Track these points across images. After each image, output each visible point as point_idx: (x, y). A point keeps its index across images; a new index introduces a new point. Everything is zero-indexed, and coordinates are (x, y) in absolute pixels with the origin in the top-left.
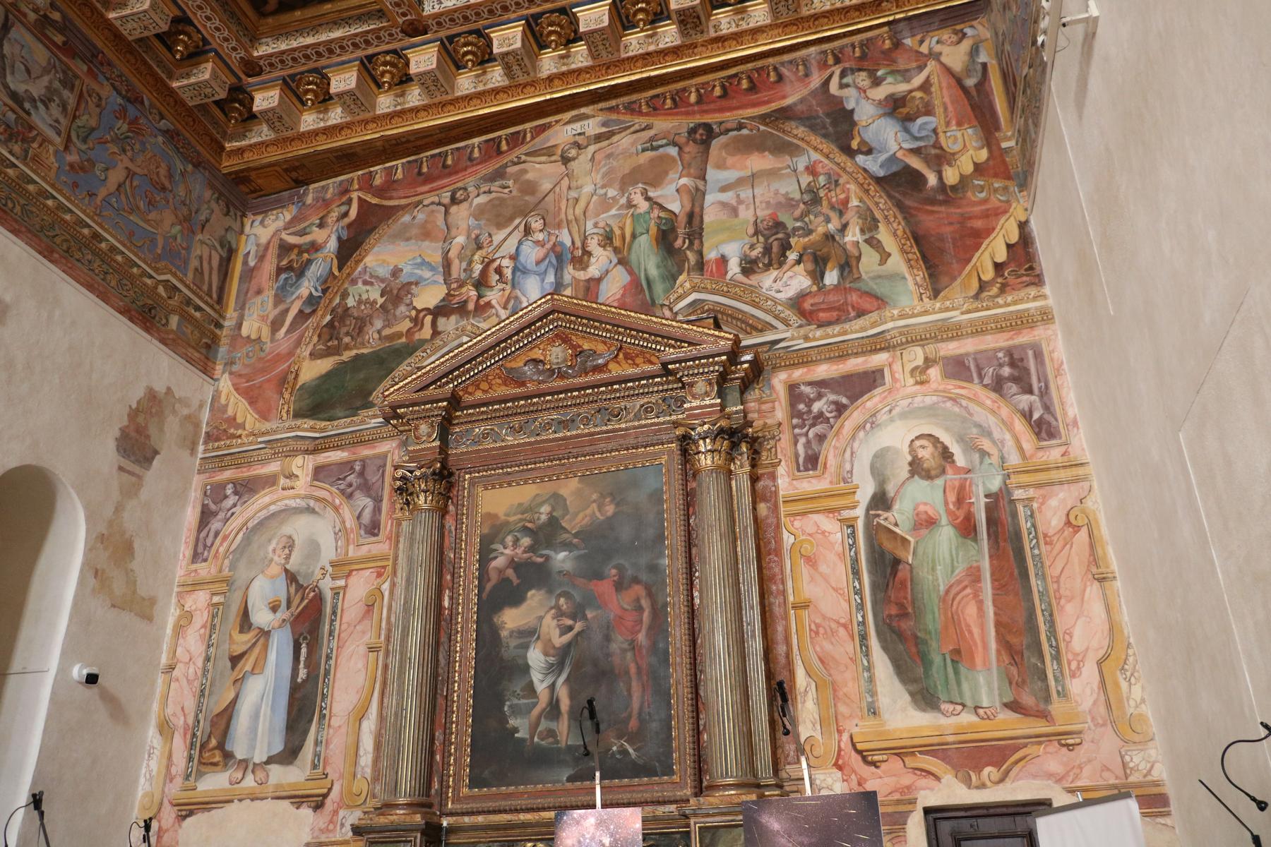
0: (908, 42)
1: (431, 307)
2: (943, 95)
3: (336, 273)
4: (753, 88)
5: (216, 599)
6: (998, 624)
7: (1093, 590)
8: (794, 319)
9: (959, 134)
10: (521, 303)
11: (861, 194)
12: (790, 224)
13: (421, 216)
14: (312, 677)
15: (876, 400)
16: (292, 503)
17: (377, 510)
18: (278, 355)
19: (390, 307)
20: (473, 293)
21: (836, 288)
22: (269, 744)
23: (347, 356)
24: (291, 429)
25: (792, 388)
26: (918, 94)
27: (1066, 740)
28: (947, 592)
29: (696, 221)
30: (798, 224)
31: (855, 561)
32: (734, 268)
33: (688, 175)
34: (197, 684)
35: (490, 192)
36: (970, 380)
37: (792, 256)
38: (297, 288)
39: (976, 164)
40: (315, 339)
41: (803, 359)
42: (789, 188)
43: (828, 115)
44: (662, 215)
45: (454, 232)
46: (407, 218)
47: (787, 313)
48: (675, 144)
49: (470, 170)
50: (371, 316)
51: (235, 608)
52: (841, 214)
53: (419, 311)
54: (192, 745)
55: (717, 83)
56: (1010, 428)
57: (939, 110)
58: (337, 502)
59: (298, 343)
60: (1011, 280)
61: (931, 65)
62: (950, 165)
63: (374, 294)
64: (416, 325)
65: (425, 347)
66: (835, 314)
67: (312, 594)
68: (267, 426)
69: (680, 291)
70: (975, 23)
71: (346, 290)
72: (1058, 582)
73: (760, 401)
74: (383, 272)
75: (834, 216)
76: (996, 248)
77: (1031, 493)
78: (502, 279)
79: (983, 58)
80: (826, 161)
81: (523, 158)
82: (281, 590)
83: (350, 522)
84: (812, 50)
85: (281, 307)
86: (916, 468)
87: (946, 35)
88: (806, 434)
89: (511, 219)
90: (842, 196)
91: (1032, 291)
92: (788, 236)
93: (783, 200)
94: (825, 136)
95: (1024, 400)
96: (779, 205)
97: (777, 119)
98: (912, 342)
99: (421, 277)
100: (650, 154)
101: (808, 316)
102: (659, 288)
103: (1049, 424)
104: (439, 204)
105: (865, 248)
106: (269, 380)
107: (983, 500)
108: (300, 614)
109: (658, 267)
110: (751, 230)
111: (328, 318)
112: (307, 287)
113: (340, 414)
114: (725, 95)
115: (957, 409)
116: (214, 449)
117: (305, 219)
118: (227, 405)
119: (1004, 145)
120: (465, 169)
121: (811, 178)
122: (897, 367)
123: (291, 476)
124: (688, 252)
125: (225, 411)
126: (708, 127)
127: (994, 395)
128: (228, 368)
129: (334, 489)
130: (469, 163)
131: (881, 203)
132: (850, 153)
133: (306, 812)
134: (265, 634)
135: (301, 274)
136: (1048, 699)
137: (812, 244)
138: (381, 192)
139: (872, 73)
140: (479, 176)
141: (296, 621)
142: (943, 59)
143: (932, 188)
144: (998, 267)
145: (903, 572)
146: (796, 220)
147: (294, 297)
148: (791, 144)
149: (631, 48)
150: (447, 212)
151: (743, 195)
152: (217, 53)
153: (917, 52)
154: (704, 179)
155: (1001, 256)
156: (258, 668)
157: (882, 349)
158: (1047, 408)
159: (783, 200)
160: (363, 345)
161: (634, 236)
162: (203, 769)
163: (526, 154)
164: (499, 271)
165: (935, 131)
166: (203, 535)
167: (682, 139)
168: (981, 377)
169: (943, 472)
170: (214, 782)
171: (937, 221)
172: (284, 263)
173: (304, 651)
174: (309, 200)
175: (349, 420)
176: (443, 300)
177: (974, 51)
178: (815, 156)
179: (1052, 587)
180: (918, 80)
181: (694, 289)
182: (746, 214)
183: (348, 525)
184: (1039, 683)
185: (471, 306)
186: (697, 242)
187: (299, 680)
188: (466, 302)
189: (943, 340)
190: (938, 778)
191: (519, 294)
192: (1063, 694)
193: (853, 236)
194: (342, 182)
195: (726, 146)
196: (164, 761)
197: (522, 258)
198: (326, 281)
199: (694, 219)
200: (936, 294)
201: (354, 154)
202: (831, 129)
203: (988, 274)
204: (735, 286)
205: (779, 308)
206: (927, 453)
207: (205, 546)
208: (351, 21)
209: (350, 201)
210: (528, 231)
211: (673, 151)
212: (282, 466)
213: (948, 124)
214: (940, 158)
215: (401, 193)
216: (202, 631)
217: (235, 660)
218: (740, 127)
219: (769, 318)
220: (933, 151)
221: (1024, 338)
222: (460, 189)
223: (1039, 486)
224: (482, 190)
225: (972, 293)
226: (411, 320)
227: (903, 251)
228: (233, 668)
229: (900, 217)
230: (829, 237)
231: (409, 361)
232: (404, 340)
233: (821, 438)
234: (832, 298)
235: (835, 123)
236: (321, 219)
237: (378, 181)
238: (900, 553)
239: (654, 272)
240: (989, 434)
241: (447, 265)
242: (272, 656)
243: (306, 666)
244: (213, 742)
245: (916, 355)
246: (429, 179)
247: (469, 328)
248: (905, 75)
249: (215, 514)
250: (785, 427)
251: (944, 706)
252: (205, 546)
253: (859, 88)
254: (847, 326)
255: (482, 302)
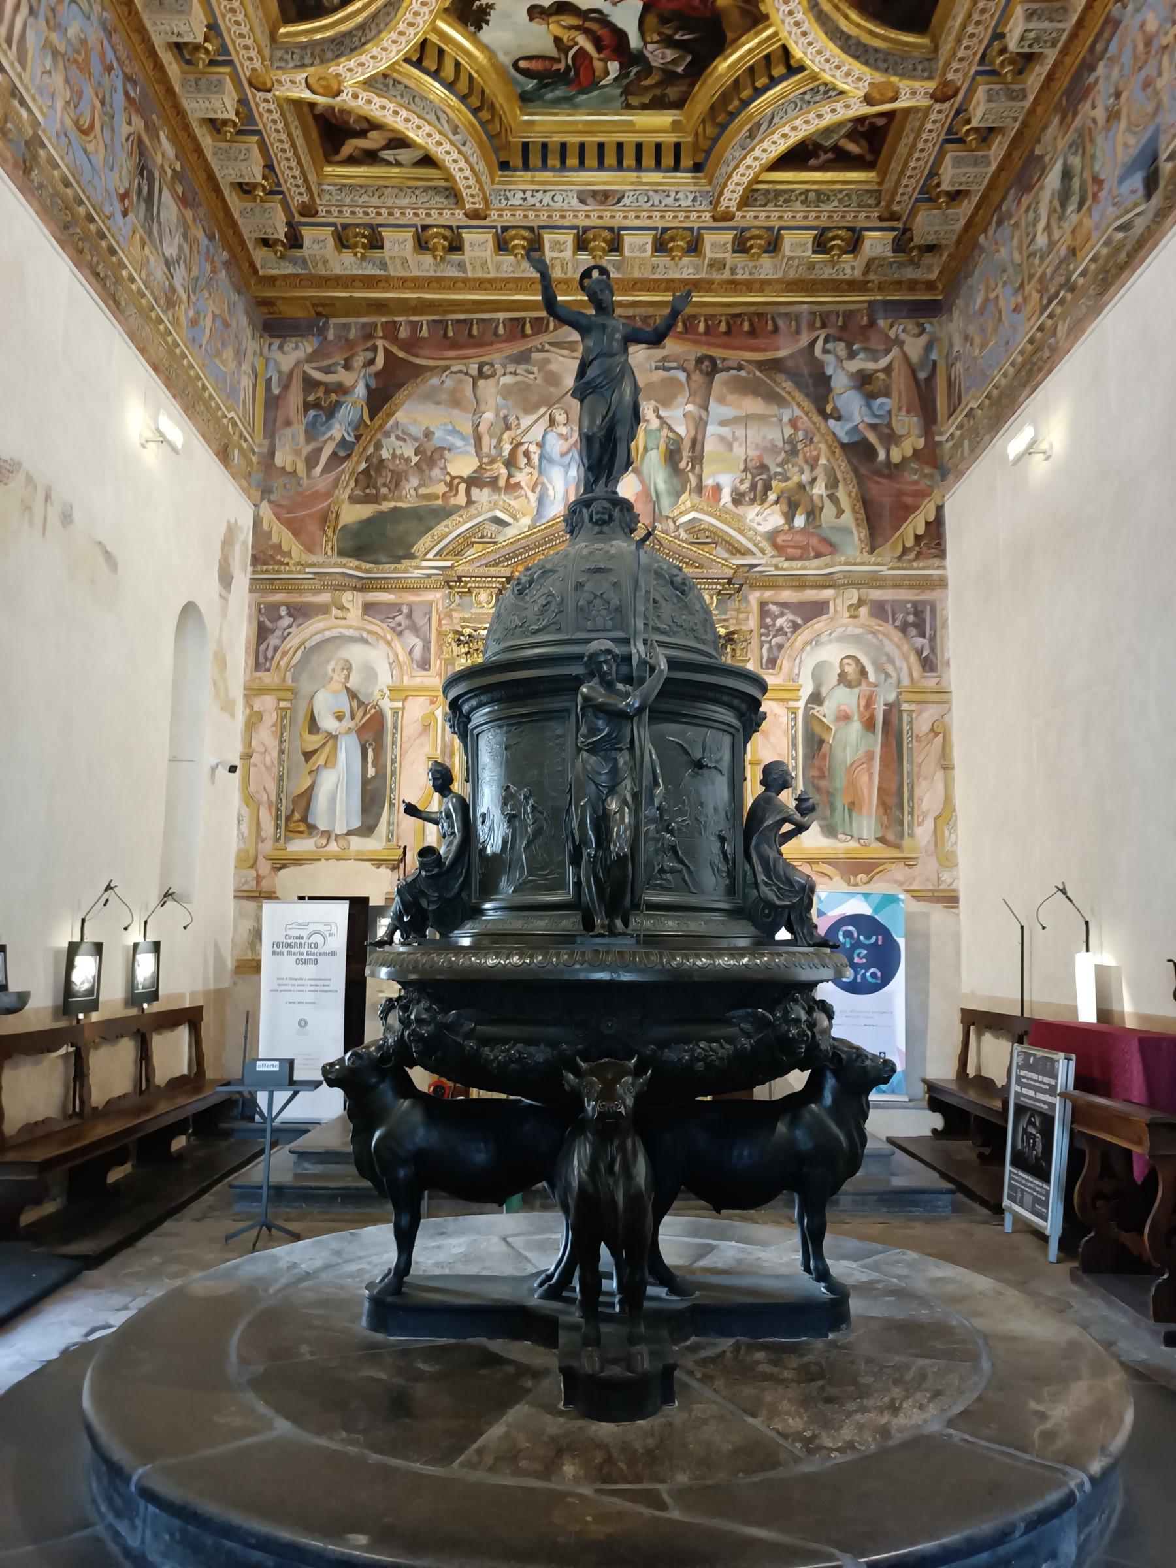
0: (881, 323)
1: (465, 475)
2: (900, 381)
3: (368, 422)
4: (753, 333)
5: (282, 704)
6: (880, 789)
7: (940, 774)
8: (769, 550)
9: (907, 420)
10: (547, 489)
11: (829, 454)
12: (774, 469)
13: (449, 383)
14: (381, 774)
15: (821, 624)
16: (348, 632)
17: (426, 648)
18: (316, 492)
19: (424, 467)
20: (504, 471)
21: (802, 531)
22: (347, 822)
23: (386, 506)
24: (336, 565)
25: (763, 604)
26: (882, 376)
27: (909, 863)
28: (851, 765)
29: (698, 448)
30: (779, 470)
31: (794, 738)
32: (726, 497)
33: (694, 403)
34: (275, 770)
35: (515, 374)
36: (886, 621)
37: (772, 497)
38: (329, 428)
39: (915, 451)
40: (352, 484)
41: (771, 583)
42: (775, 435)
43: (811, 376)
44: (671, 435)
45: (482, 407)
46: (435, 381)
47: (765, 544)
48: (684, 370)
49: (495, 346)
50: (406, 473)
51: (302, 715)
52: (812, 469)
53: (453, 478)
54: (278, 817)
55: (723, 318)
56: (906, 659)
57: (895, 395)
58: (389, 637)
59: (336, 484)
60: (925, 550)
61: (895, 351)
62: (897, 445)
63: (408, 451)
64: (451, 490)
65: (461, 512)
66: (799, 552)
67: (373, 711)
68: (313, 559)
69: (683, 508)
70: (934, 320)
71: (379, 441)
72: (920, 765)
73: (738, 611)
74: (416, 431)
75: (807, 469)
76: (917, 524)
77: (913, 706)
78: (529, 462)
79: (934, 356)
80: (805, 418)
81: (547, 347)
82: (344, 704)
83: (402, 656)
84: (805, 307)
85: (313, 445)
86: (842, 678)
87: (911, 325)
88: (770, 642)
89: (537, 407)
90: (815, 453)
91: (937, 562)
92: (770, 479)
93: (769, 445)
94: (807, 395)
95: (920, 641)
96: (765, 448)
97: (770, 369)
98: (852, 584)
99: (453, 444)
100: (661, 373)
101: (779, 549)
102: (665, 502)
103: (932, 661)
104: (467, 374)
105: (827, 502)
106: (310, 515)
107: (883, 708)
108: (364, 725)
109: (665, 482)
110: (742, 467)
111: (363, 465)
112: (338, 430)
113: (384, 560)
114: (728, 332)
115: (874, 641)
116: (262, 572)
117: (327, 356)
118: (270, 532)
119: (937, 439)
120: (491, 344)
121: (792, 431)
122: (839, 602)
123: (342, 608)
124: (690, 475)
125: (270, 538)
126: (712, 360)
127: (900, 635)
128: (266, 495)
129: (384, 626)
130: (494, 338)
131: (842, 467)
132: (825, 416)
133: (384, 871)
134: (333, 738)
135: (331, 412)
136: (902, 836)
137: (789, 489)
138: (407, 346)
139: (849, 346)
140: (505, 354)
141: (361, 730)
142: (906, 348)
143: (881, 462)
144: (918, 538)
145: (825, 747)
146: (780, 465)
147: (326, 436)
148: (779, 395)
149: (659, 270)
150: (475, 384)
151: (737, 434)
152: (285, 197)
153: (887, 336)
154: (706, 409)
155: (920, 531)
156: (330, 762)
157: (829, 587)
158: (933, 650)
159: (769, 445)
160: (400, 499)
161: (646, 450)
162: (291, 835)
163: (551, 344)
164: (527, 454)
165: (889, 412)
166: (263, 647)
167: (691, 366)
168: (894, 620)
169: (860, 684)
170: (301, 845)
171: (881, 490)
172: (311, 398)
173: (370, 754)
174: (331, 335)
175: (393, 566)
176: (475, 472)
177: (929, 348)
178: (798, 412)
179: (916, 769)
180: (883, 362)
181: (694, 508)
182: (739, 451)
183: (401, 658)
184: (899, 828)
185: (502, 483)
186: (698, 467)
187: (369, 776)
188: (497, 478)
189: (872, 587)
190: (831, 878)
191: (546, 481)
192: (911, 835)
193: (819, 490)
194: (364, 325)
195: (726, 383)
196: (254, 827)
197: (548, 447)
198: (357, 428)
199: (696, 443)
200: (872, 550)
201: (386, 306)
202: (812, 389)
203: (910, 543)
204: (726, 513)
205: (759, 538)
206: (850, 669)
207: (266, 658)
208: (417, 192)
209: (374, 349)
210: (552, 422)
211: (682, 376)
212: (333, 599)
213: (900, 409)
214: (890, 438)
215: (426, 352)
216: (274, 729)
217: (308, 755)
218: (740, 368)
219: (750, 546)
220: (886, 431)
221: (926, 596)
222: (487, 363)
223: (918, 703)
224: (508, 370)
225: (898, 554)
226: (446, 484)
227: (854, 511)
228: (307, 761)
229: (855, 482)
230: (801, 487)
231: (446, 522)
232: (440, 502)
233: (780, 647)
234: (798, 538)
235: (816, 385)
236: (346, 360)
237: (403, 333)
238: (824, 736)
239: (662, 486)
240: (892, 661)
241: (478, 439)
242: (342, 756)
243: (375, 765)
244: (297, 816)
245: (853, 595)
246: (455, 345)
247: (501, 503)
248: (874, 355)
249: (273, 631)
250: (755, 634)
251: (840, 836)
252: (266, 658)
253: (837, 357)
254: (807, 563)
255: (512, 481)
